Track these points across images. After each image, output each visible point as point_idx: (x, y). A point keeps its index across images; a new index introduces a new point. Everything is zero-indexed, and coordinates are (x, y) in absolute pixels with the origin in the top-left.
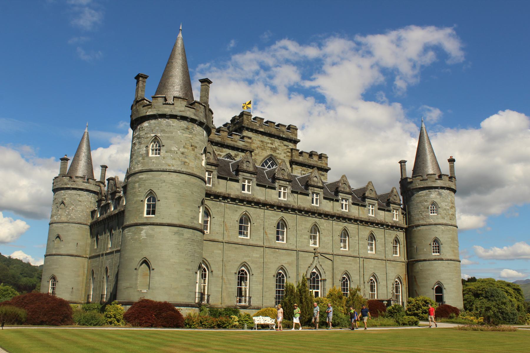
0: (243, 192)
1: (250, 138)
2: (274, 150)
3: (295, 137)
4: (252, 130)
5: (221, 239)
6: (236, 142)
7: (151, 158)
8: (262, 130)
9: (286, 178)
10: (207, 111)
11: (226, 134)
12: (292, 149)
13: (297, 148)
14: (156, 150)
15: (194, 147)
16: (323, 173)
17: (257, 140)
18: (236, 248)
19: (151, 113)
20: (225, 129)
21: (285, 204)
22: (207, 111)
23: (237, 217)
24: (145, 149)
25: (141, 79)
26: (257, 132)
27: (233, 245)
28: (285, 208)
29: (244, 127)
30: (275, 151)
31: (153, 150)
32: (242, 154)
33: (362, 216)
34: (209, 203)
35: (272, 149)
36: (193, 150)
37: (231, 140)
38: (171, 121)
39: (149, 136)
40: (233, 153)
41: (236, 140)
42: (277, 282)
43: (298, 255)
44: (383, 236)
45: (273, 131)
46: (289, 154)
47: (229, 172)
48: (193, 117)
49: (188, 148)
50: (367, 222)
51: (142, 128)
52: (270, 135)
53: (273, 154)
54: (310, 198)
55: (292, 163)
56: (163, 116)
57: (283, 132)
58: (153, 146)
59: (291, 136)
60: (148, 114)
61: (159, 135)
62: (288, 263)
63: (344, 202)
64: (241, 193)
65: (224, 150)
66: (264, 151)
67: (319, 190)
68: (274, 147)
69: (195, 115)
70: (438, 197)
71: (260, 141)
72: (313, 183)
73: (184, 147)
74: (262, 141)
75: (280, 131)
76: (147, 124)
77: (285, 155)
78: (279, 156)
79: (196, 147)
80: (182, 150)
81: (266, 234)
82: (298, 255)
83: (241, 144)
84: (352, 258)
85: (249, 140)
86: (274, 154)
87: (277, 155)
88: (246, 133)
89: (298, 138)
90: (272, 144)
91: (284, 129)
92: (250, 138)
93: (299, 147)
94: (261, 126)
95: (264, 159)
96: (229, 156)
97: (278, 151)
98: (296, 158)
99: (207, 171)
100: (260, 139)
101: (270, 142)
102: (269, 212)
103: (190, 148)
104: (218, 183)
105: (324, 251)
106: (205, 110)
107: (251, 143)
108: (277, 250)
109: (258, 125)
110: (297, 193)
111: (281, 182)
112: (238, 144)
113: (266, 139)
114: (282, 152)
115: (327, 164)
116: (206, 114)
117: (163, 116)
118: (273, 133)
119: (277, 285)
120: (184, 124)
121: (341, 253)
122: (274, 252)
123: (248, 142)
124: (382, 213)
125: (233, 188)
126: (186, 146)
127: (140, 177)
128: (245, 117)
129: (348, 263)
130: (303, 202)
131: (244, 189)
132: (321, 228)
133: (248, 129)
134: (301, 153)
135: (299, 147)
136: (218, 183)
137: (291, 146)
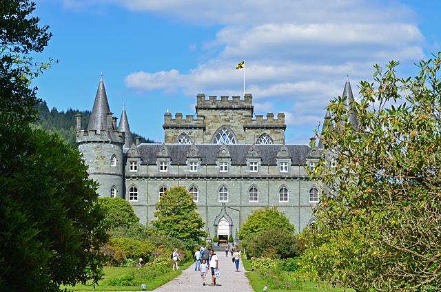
1: (201, 116)
4: (205, 109)
5: (145, 203)
8: (214, 107)
9: (196, 156)
12: (245, 116)
15: (103, 158)
16: (278, 131)
23: (158, 189)
26: (209, 109)
28: (195, 178)
30: (229, 121)
32: (194, 131)
33: (273, 174)
35: (225, 120)
38: (88, 145)
43: (207, 209)
44: (297, 187)
45: (226, 104)
46: (242, 120)
50: (276, 178)
55: (245, 128)
56: (84, 142)
59: (245, 104)
63: (254, 165)
64: (159, 172)
65: (179, 130)
72: (220, 155)
78: (232, 125)
80: (95, 161)
82: (207, 209)
90: (226, 116)
97: (231, 121)
100: (214, 114)
110: (205, 165)
112: (191, 124)
115: (283, 122)
117: (84, 142)
120: (95, 145)
121: (250, 204)
124: (296, 168)
125: (153, 170)
130: (210, 170)
132: (229, 187)
137: (247, 113)
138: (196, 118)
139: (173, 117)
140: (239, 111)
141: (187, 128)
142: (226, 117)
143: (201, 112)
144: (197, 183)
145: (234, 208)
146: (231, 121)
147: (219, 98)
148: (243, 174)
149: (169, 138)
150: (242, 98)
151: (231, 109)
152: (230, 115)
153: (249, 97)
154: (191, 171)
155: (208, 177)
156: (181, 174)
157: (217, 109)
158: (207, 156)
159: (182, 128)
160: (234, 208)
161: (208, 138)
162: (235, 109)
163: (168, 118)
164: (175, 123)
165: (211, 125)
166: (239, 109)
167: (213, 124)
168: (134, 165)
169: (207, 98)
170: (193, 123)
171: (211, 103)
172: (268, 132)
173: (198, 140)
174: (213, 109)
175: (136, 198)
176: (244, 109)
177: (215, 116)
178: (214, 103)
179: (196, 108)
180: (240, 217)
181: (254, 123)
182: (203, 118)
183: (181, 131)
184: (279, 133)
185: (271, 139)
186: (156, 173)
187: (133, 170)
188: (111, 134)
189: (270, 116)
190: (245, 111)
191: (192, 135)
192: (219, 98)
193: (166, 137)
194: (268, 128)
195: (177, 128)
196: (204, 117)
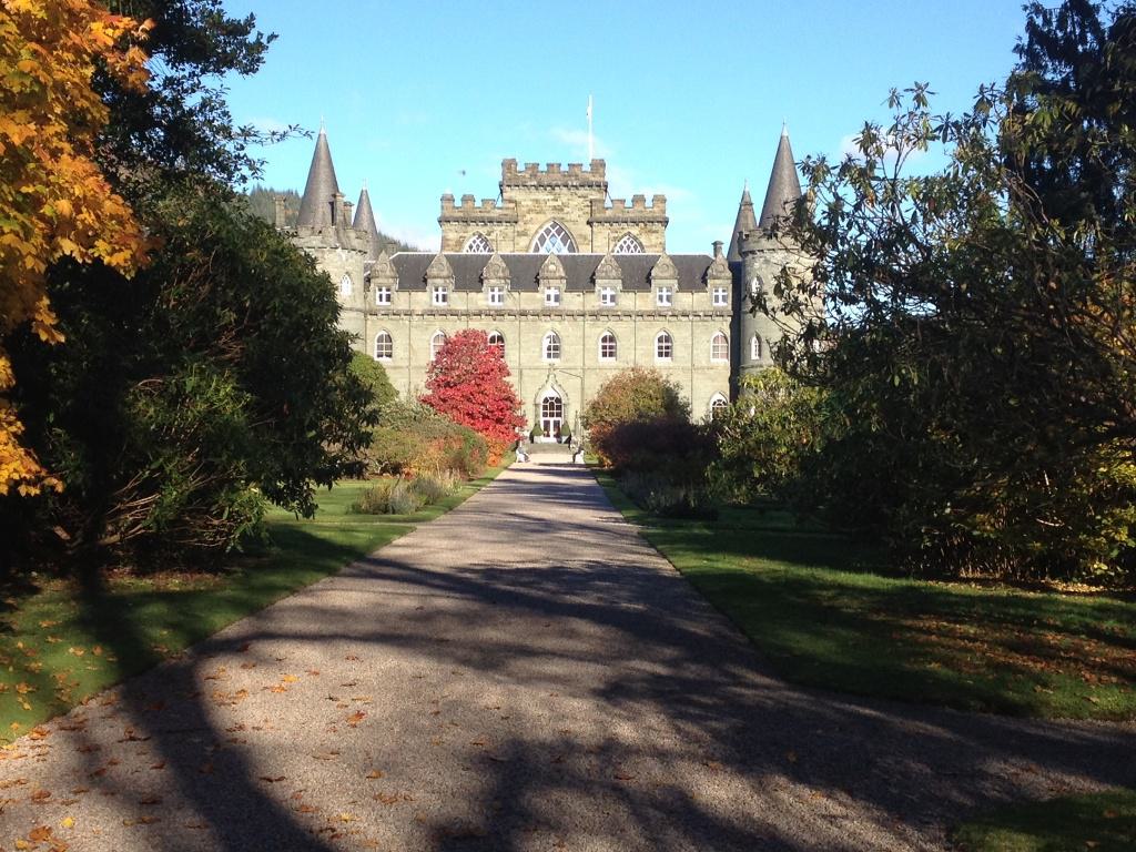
1: (510, 201)
8: (535, 183)
28: (500, 314)
30: (562, 210)
32: (498, 229)
33: (643, 309)
35: (555, 208)
45: (556, 178)
48: (321, 245)
53: (556, 215)
65: (469, 228)
67: (558, 281)
70: (764, 266)
77: (581, 213)
78: (568, 218)
86: (561, 215)
87: (564, 216)
89: (606, 179)
95: (541, 227)
97: (566, 210)
100: (533, 197)
112: (492, 215)
113: (542, 195)
114: (575, 207)
132: (562, 334)
135: (614, 193)
137: (594, 195)
138: (499, 204)
139: (458, 203)
140: (582, 191)
142: (556, 204)
143: (509, 193)
144: (506, 327)
145: (573, 372)
146: (566, 210)
147: (543, 168)
148: (588, 308)
149: (450, 243)
150: (587, 168)
151: (566, 186)
152: (564, 199)
153: (598, 165)
154: (715, 304)
155: (523, 314)
156: (473, 308)
157: (539, 186)
158: (526, 274)
160: (573, 372)
161: (523, 242)
163: (447, 204)
164: (461, 214)
165: (528, 217)
167: (533, 215)
168: (384, 293)
169: (521, 167)
170: (495, 214)
171: (527, 176)
172: (635, 231)
173: (507, 244)
175: (390, 356)
177: (537, 201)
178: (534, 176)
179: (501, 186)
180: (583, 389)
181: (609, 213)
182: (512, 205)
183: (473, 228)
184: (656, 232)
185: (641, 244)
186: (426, 307)
187: (384, 303)
188: (341, 235)
189: (639, 199)
190: (594, 193)
191: (493, 236)
192: (543, 168)
193: (444, 239)
194: (635, 222)
196: (515, 202)
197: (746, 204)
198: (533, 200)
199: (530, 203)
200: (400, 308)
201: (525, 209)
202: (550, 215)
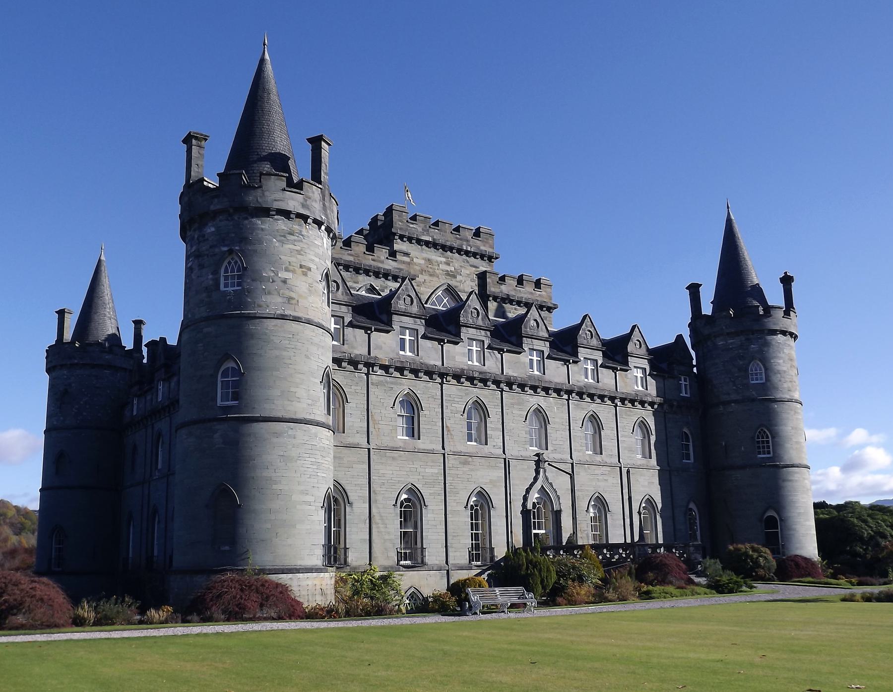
0: (402, 353)
1: (407, 254)
2: (452, 275)
3: (491, 250)
4: (410, 240)
6: (382, 262)
7: (225, 294)
10: (327, 198)
11: (362, 248)
13: (495, 271)
14: (233, 277)
17: (419, 256)
18: (394, 458)
19: (218, 207)
20: (360, 238)
21: (480, 373)
22: (327, 198)
24: (210, 276)
25: (194, 141)
26: (419, 242)
27: (389, 453)
29: (395, 234)
30: (455, 277)
31: (226, 278)
34: (339, 377)
36: (305, 274)
37: (373, 260)
39: (217, 250)
40: (377, 283)
41: (380, 258)
42: (472, 519)
45: (450, 239)
47: (374, 314)
49: (294, 272)
51: (204, 236)
52: (445, 248)
54: (524, 358)
57: (468, 241)
58: (226, 271)
59: (482, 248)
60: (212, 208)
61: (237, 248)
62: (491, 482)
66: (435, 279)
68: (453, 269)
69: (304, 206)
71: (425, 259)
73: (287, 270)
74: (429, 260)
75: (461, 239)
76: (213, 229)
78: (461, 287)
79: (310, 269)
81: (449, 431)
83: (390, 265)
84: (609, 469)
85: (406, 259)
86: (453, 283)
87: (458, 284)
88: (398, 245)
91: (469, 235)
92: (407, 254)
93: (498, 267)
94: (426, 231)
96: (372, 289)
97: (459, 278)
98: (493, 289)
99: (333, 316)
100: (425, 255)
101: (444, 260)
102: (451, 388)
103: (299, 271)
104: (355, 337)
105: (558, 456)
106: (324, 196)
107: (409, 264)
108: (470, 459)
109: (420, 229)
111: (471, 331)
113: (436, 256)
116: (324, 205)
118: (448, 244)
119: (472, 524)
122: (465, 463)
123: (404, 262)
126: (291, 268)
127: (205, 330)
128: (395, 215)
129: (601, 477)
131: (403, 348)
133: (402, 237)
134: (502, 279)
135: (498, 267)
136: (355, 337)
137: (483, 266)
141: (377, 274)
151: (459, 251)
159: (367, 272)
162: (467, 253)
164: (351, 259)
166: (475, 255)
174: (427, 244)
176: (482, 257)
195: (357, 270)
197: (694, 290)
198: (425, 259)
199: (423, 262)
200: (357, 352)
201: (418, 268)
202: (444, 280)
